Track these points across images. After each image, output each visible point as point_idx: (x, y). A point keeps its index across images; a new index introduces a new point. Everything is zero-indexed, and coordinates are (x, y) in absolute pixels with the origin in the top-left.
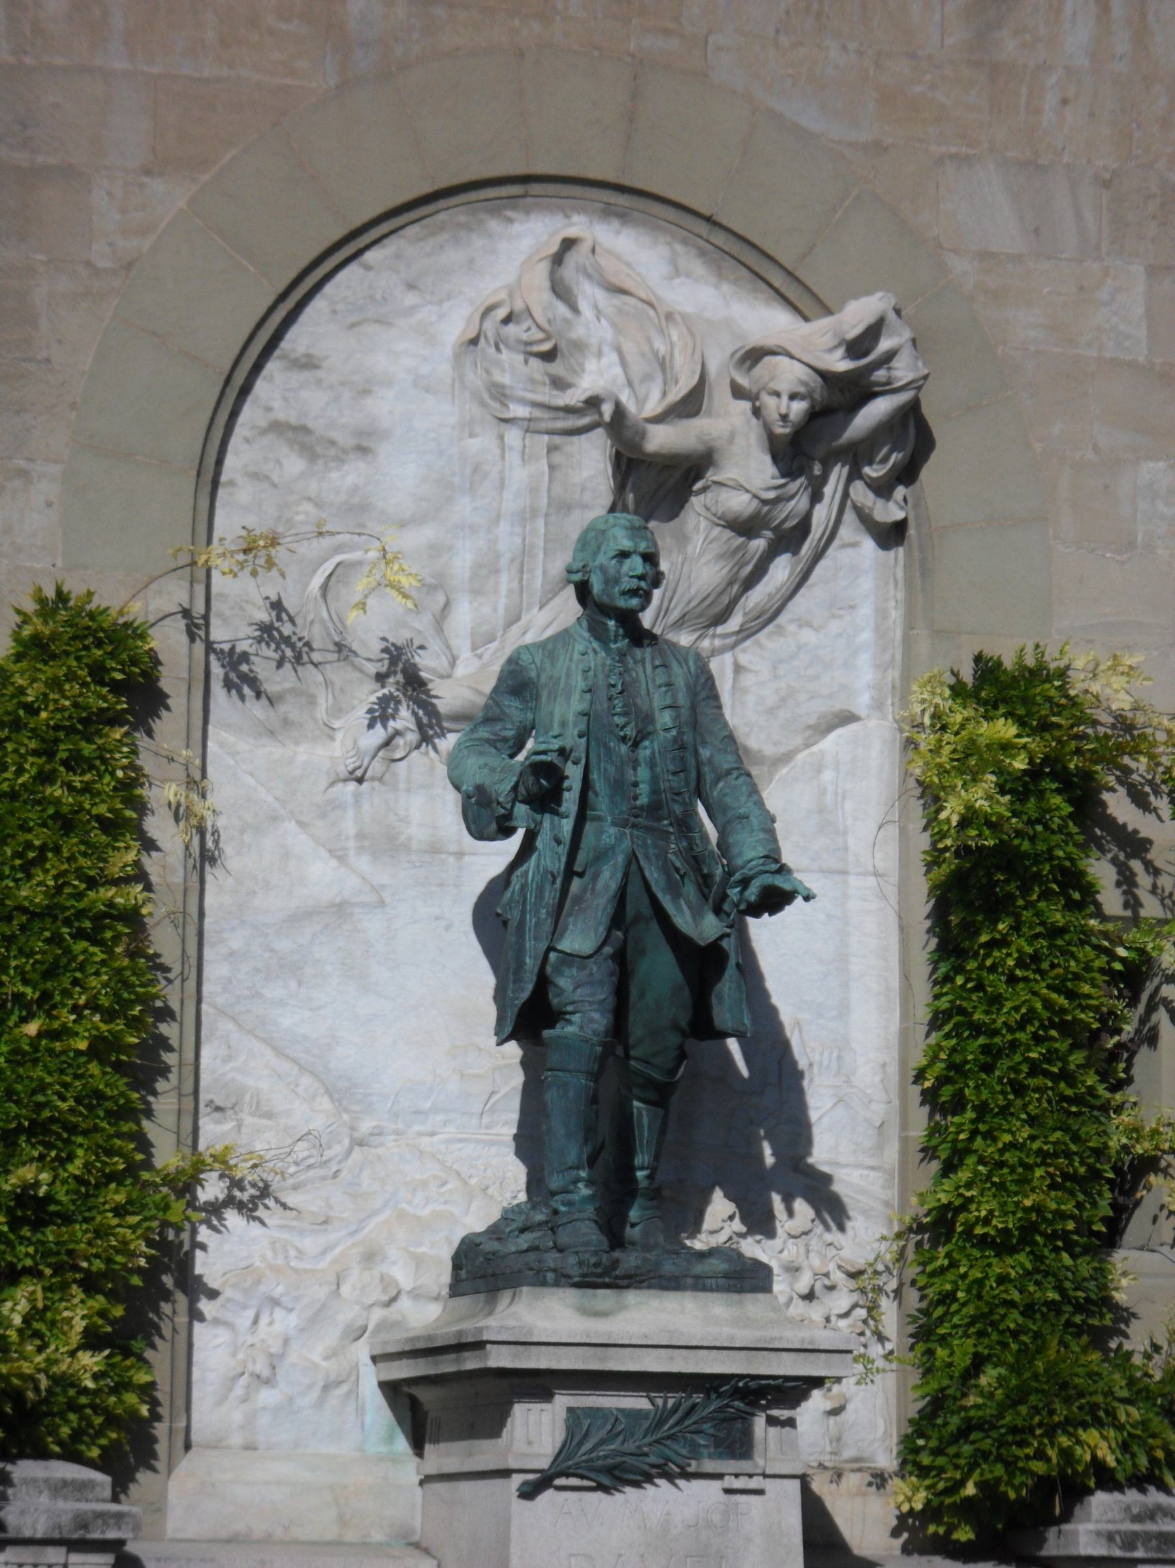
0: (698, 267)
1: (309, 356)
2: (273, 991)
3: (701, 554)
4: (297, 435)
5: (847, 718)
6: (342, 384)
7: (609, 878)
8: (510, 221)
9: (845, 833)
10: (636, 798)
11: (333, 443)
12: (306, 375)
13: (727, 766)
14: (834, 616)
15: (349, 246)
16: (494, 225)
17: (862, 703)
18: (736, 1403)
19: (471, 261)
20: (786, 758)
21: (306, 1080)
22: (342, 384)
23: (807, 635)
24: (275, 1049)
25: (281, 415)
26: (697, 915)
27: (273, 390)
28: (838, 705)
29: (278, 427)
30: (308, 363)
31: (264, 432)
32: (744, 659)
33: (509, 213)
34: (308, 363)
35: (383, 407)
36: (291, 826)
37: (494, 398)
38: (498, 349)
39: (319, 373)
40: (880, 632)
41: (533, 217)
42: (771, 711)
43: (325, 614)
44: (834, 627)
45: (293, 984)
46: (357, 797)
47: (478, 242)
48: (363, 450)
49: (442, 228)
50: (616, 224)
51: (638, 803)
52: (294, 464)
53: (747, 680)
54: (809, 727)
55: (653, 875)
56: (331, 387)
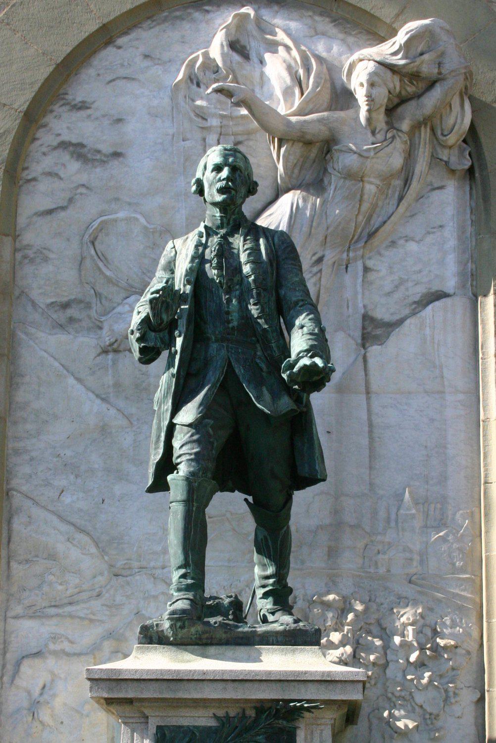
0: (332, 29)
1: (83, 102)
2: (60, 482)
3: (333, 197)
4: (78, 151)
5: (440, 296)
6: (104, 116)
7: (214, 375)
8: (208, 12)
9: (441, 367)
10: (229, 322)
11: (99, 152)
12: (83, 114)
13: (294, 299)
14: (429, 233)
15: (106, 36)
16: (197, 15)
17: (450, 284)
18: (280, 721)
19: (183, 37)
20: (401, 322)
21: (80, 536)
22: (104, 116)
23: (412, 246)
24: (60, 517)
25: (66, 137)
26: (275, 397)
27: (63, 125)
28: (435, 288)
29: (64, 145)
30: (83, 106)
31: (55, 148)
32: (370, 264)
33: (207, 8)
34: (83, 106)
35: (131, 128)
36: (71, 381)
37: (197, 115)
38: (198, 85)
39: (89, 112)
40: (461, 239)
41: (221, 8)
42: (389, 294)
43: (93, 252)
44: (429, 239)
45: (72, 477)
46: (115, 362)
47: (186, 25)
48: (117, 155)
49: (165, 20)
50: (276, 8)
51: (231, 325)
52: (74, 166)
53: (371, 276)
54: (415, 302)
55: (239, 370)
56: (97, 118)
